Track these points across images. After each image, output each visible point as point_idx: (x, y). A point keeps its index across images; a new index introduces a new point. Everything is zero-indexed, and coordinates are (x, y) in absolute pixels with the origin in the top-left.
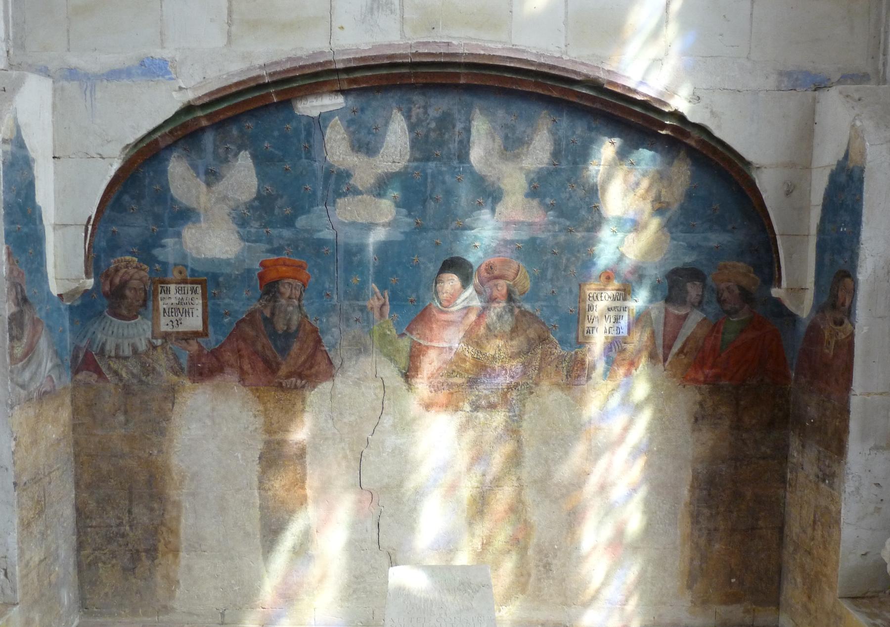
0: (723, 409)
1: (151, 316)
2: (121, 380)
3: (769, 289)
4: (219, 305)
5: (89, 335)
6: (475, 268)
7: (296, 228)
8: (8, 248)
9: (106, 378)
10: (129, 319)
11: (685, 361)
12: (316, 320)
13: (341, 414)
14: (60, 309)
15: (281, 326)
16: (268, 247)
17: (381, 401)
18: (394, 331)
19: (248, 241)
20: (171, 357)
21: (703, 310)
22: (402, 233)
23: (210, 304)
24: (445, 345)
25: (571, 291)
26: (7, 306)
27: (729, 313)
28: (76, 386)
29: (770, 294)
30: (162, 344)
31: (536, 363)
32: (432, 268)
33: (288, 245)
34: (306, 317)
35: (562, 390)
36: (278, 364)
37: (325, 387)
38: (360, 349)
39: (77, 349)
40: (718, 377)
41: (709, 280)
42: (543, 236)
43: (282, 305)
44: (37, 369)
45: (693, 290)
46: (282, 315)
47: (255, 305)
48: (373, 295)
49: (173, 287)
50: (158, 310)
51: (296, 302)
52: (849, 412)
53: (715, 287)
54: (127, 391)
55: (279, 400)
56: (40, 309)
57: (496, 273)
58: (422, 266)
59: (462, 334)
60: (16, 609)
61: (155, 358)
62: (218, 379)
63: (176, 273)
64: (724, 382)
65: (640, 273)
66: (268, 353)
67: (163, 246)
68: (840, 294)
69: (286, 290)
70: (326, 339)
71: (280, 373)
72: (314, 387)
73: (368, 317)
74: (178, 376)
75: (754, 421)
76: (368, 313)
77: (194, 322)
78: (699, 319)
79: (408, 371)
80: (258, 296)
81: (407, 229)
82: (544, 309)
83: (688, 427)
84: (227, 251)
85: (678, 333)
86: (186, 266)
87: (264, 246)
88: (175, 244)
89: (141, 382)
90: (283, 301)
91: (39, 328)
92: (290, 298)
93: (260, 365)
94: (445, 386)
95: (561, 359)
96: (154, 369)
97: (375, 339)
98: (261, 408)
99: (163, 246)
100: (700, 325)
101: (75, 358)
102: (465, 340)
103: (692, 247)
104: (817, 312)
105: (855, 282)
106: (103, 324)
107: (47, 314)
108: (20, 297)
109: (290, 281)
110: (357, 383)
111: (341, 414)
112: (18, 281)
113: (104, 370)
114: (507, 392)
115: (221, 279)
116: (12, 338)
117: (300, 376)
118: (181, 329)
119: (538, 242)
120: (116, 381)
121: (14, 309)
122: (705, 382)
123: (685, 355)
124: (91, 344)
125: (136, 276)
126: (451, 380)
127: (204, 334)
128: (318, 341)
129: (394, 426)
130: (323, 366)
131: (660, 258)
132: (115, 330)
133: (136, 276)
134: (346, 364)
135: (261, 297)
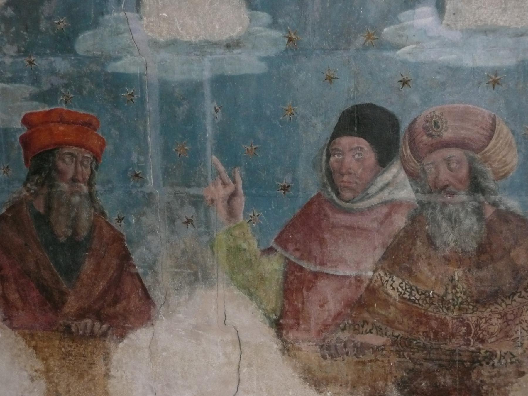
6: (404, 126)
7: (76, 54)
12: (120, 220)
13: (168, 385)
15: (63, 231)
16: (33, 89)
17: (235, 368)
18: (255, 244)
22: (262, 59)
24: (349, 272)
32: (320, 127)
33: (66, 86)
34: (103, 214)
36: (63, 294)
37: (140, 336)
38: (195, 273)
43: (62, 193)
47: (18, 191)
48: (214, 177)
51: (85, 189)
55: (68, 354)
57: (447, 135)
59: (379, 253)
66: (46, 274)
69: (67, 167)
70: (138, 255)
71: (66, 310)
72: (122, 337)
73: (206, 216)
76: (207, 209)
79: (281, 317)
80: (24, 176)
81: (272, 52)
87: (26, 89)
90: (64, 186)
92: (74, 180)
94: (349, 349)
98: (40, 366)
102: (386, 264)
109: (73, 149)
110: (195, 333)
111: (168, 385)
114: (471, 368)
117: (99, 317)
126: (360, 339)
128: (125, 258)
130: (135, 301)
134: (173, 299)
135: (28, 180)
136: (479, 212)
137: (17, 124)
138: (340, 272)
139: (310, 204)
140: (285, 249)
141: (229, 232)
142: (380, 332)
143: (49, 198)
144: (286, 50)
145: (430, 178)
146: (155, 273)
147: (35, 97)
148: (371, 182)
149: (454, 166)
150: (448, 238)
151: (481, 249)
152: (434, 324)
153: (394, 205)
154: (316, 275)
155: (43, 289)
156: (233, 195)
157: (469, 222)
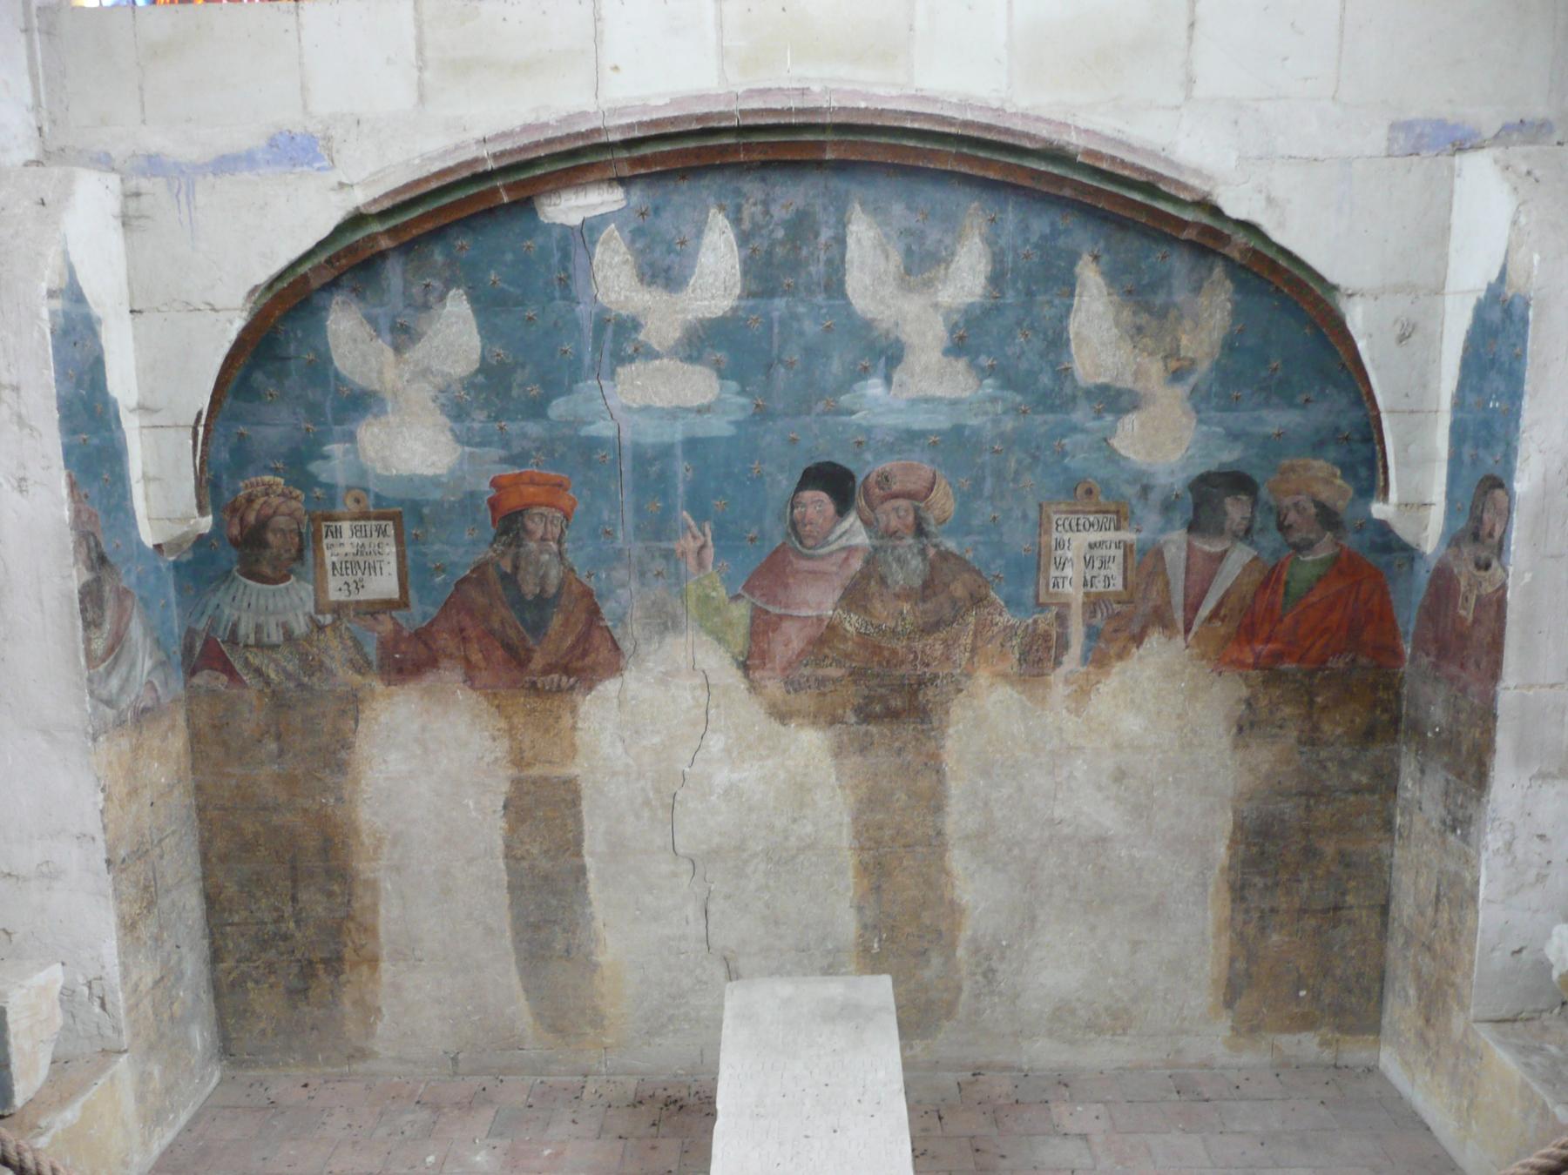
0: (1287, 711)
1: (311, 576)
2: (268, 683)
3: (1367, 504)
4: (425, 555)
5: (209, 611)
6: (859, 480)
8: (69, 476)
9: (242, 682)
10: (275, 582)
11: (1222, 631)
12: (589, 576)
14: (158, 569)
15: (530, 588)
16: (502, 453)
18: (723, 592)
19: (468, 444)
20: (350, 643)
21: (1252, 543)
23: (409, 553)
24: (810, 613)
25: (1025, 517)
26: (74, 573)
27: (1299, 548)
28: (193, 694)
29: (1370, 514)
30: (334, 622)
31: (966, 640)
32: (785, 482)
33: (538, 449)
34: (572, 570)
35: (1012, 684)
36: (529, 651)
37: (610, 687)
38: (666, 623)
39: (191, 633)
40: (1279, 656)
41: (1264, 492)
42: (974, 422)
44: (129, 672)
45: (1236, 510)
46: (531, 569)
47: (484, 553)
49: (346, 526)
50: (323, 564)
51: (554, 546)
52: (1495, 717)
53: (1273, 503)
54: (279, 702)
55: (534, 710)
56: (129, 571)
57: (896, 487)
58: (768, 479)
59: (838, 594)
60: (123, 1059)
61: (322, 645)
62: (429, 678)
63: (350, 503)
64: (1288, 666)
65: (1145, 481)
66: (511, 633)
67: (326, 457)
68: (1486, 516)
69: (536, 526)
70: (608, 608)
71: (532, 666)
72: (590, 689)
74: (363, 675)
75: (1339, 731)
76: (677, 561)
77: (385, 584)
78: (1247, 559)
79: (748, 658)
80: (490, 538)
81: (740, 416)
82: (981, 548)
83: (1226, 742)
84: (433, 464)
85: (1210, 582)
86: (366, 490)
87: (495, 452)
88: (346, 452)
89: (301, 685)
90: (532, 545)
91: (128, 603)
92: (543, 539)
93: (499, 654)
95: (1010, 631)
96: (322, 664)
97: (692, 602)
98: (503, 724)
99: (326, 457)
100: (1247, 569)
101: (188, 649)
102: (844, 603)
103: (1234, 436)
104: (1449, 546)
105: (1510, 495)
106: (232, 591)
107: (139, 579)
108: (94, 555)
109: (543, 510)
110: (665, 679)
112: (89, 528)
113: (238, 666)
114: (919, 689)
115: (426, 511)
116: (88, 625)
117: (567, 670)
118: (363, 596)
119: (967, 433)
120: (261, 685)
121: (87, 576)
122: (1255, 666)
123: (1223, 620)
124: (213, 627)
125: (283, 509)
126: (821, 672)
127: (402, 603)
128: (594, 612)
129: (728, 750)
130: (605, 654)
131: (1179, 455)
132: (253, 602)
133: (283, 509)
134: (643, 648)
136: (923, 552)
137: (485, 486)
138: (804, 613)
139: (776, 552)
140: (752, 595)
141: (699, 582)
142: (839, 664)
143: (517, 557)
144: (754, 414)
145: (882, 525)
146: (625, 625)
147: (503, 461)
148: (831, 531)
149: (902, 513)
150: (898, 577)
151: (926, 585)
152: (886, 653)
153: (850, 550)
154: (781, 617)
155: (508, 647)
156: (703, 547)
157: (916, 563)
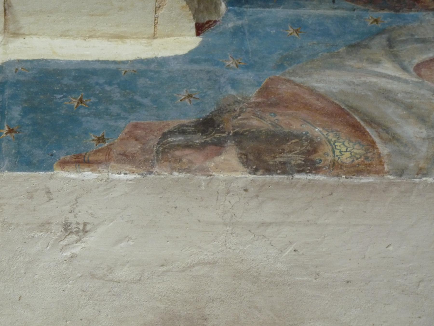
8: (64, 164)
14: (237, 32)
26: (222, 176)
44: (395, 101)
56: (234, 83)
91: (284, 89)
107: (248, 67)
108: (198, 139)
112: (153, 141)
116: (310, 166)
121: (230, 155)
